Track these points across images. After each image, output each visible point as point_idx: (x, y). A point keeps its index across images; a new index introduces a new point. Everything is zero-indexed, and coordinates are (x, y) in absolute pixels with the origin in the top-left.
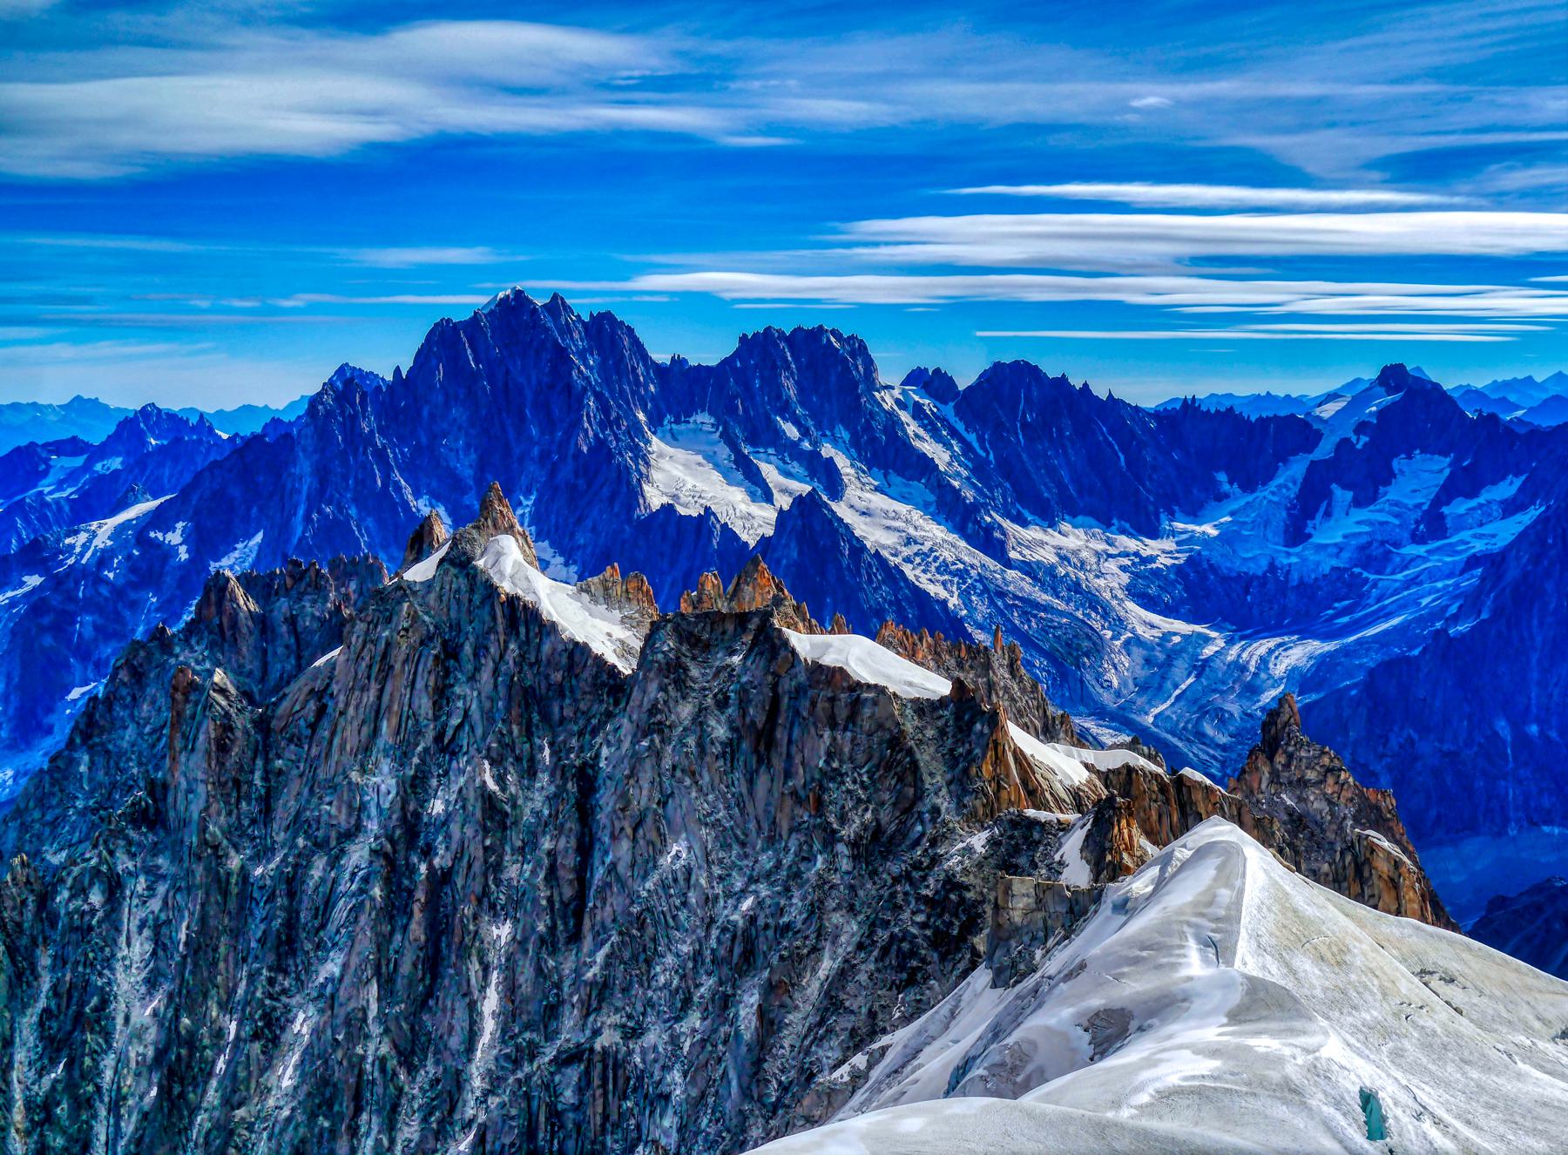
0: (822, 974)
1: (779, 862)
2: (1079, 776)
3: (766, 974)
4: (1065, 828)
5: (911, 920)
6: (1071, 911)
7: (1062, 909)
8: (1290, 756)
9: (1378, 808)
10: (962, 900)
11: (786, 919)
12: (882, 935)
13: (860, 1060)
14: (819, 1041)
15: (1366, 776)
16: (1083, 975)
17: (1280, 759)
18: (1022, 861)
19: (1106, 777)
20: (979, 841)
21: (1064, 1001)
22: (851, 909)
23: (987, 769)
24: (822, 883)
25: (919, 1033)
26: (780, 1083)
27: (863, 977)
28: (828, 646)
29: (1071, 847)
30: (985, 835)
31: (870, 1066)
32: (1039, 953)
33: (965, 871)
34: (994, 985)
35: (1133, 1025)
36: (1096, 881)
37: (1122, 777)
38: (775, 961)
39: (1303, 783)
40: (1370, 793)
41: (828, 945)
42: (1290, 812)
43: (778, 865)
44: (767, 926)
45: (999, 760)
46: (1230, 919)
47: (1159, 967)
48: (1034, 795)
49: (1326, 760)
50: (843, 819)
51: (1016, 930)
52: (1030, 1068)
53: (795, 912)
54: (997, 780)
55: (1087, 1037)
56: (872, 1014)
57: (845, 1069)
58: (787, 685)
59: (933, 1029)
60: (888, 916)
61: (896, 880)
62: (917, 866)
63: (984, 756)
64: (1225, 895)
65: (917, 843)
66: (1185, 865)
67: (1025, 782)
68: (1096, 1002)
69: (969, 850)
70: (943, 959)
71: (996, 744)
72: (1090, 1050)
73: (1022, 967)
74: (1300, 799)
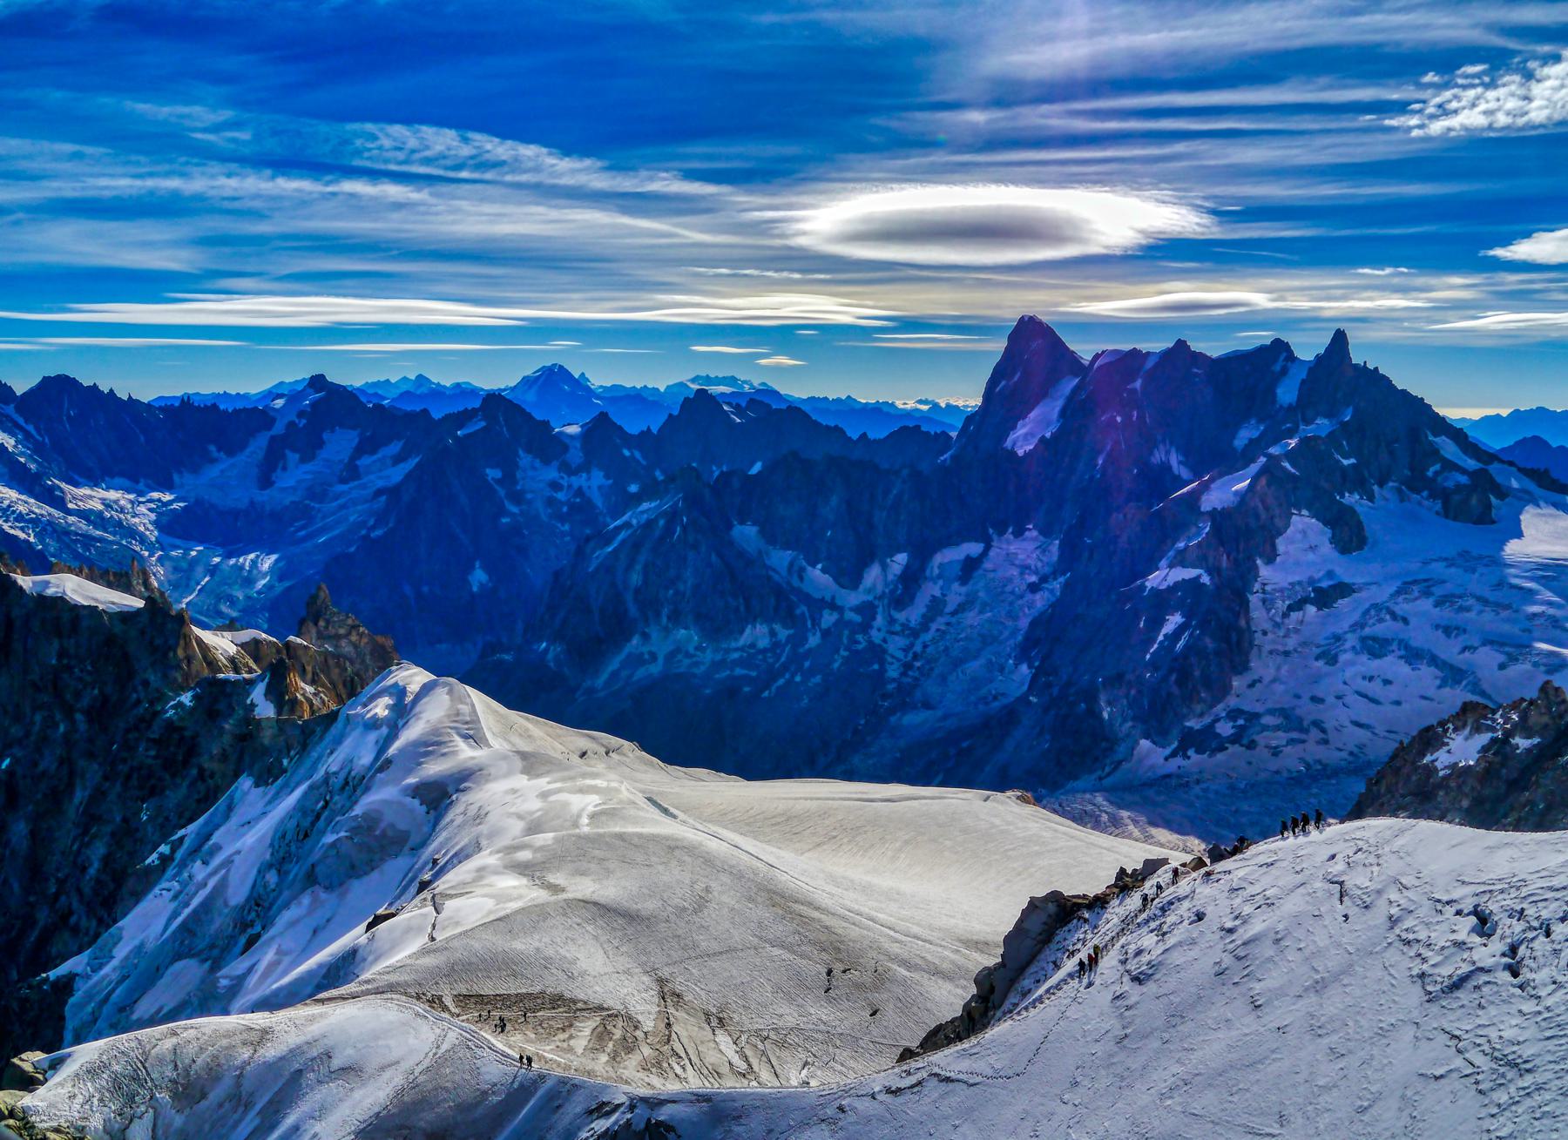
0: (76, 801)
1: (27, 735)
2: (232, 650)
3: (31, 807)
4: (251, 683)
5: (145, 754)
6: (303, 732)
7: (297, 732)
8: (328, 622)
9: (383, 647)
10: (182, 738)
11: (41, 768)
12: (123, 768)
13: (164, 849)
14: (88, 845)
15: (375, 630)
16: (393, 767)
17: (322, 623)
18: (222, 706)
19: (243, 646)
20: (186, 698)
21: (384, 784)
22: (91, 755)
23: (180, 653)
24: (67, 741)
25: (206, 823)
26: (57, 879)
27: (112, 796)
28: (47, 583)
29: (258, 694)
30: (190, 694)
31: (173, 851)
32: (285, 762)
33: (181, 719)
34: (257, 785)
35: (450, 789)
36: (279, 713)
37: (252, 646)
38: (39, 796)
39: (338, 637)
40: (380, 639)
41: (78, 781)
42: (333, 655)
43: (27, 735)
44: (24, 777)
45: (188, 645)
46: (474, 721)
47: (444, 755)
48: (212, 663)
49: (350, 622)
50: (78, 695)
51: (266, 751)
52: (383, 825)
53: (48, 763)
54: (189, 660)
55: (416, 802)
56: (125, 820)
57: (154, 856)
58: (16, 612)
59: (216, 820)
60: (124, 754)
61: (128, 731)
62: (142, 720)
63: (177, 644)
64: (464, 708)
65: (139, 702)
66: (419, 697)
67: (205, 657)
68: (412, 780)
69: (180, 704)
70: (174, 776)
71: (187, 637)
72: (424, 808)
73: (275, 771)
74: (336, 647)
